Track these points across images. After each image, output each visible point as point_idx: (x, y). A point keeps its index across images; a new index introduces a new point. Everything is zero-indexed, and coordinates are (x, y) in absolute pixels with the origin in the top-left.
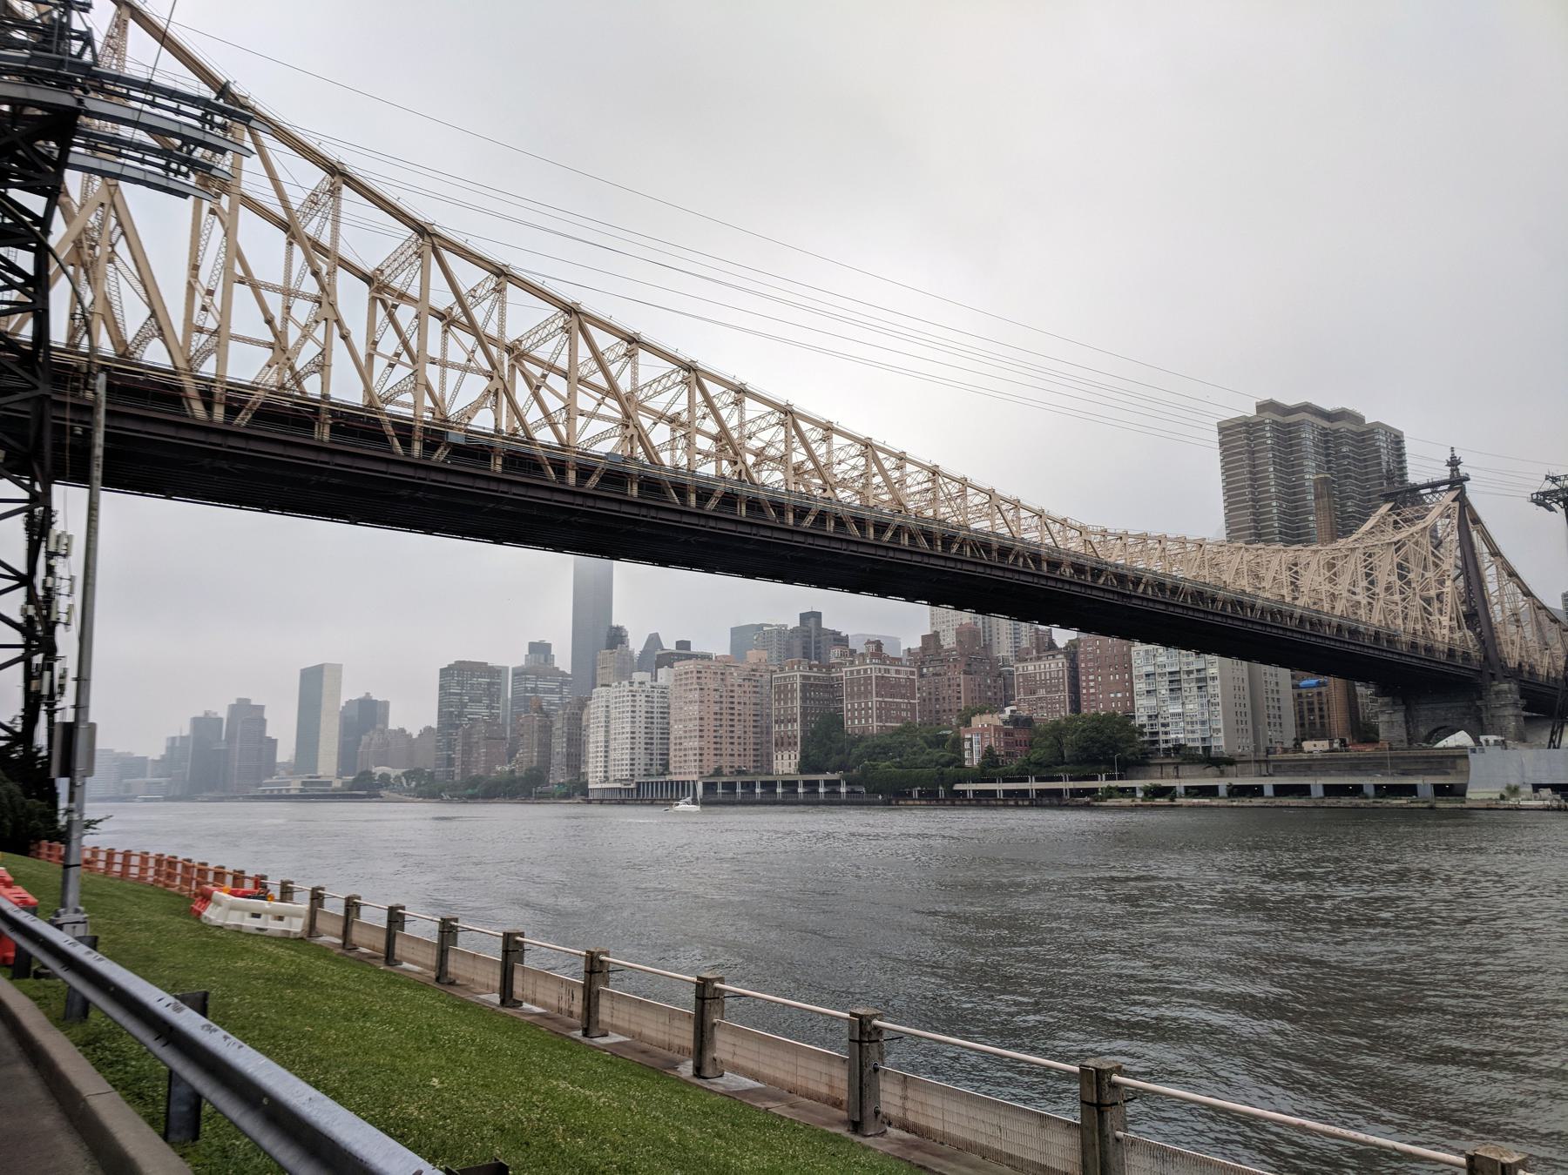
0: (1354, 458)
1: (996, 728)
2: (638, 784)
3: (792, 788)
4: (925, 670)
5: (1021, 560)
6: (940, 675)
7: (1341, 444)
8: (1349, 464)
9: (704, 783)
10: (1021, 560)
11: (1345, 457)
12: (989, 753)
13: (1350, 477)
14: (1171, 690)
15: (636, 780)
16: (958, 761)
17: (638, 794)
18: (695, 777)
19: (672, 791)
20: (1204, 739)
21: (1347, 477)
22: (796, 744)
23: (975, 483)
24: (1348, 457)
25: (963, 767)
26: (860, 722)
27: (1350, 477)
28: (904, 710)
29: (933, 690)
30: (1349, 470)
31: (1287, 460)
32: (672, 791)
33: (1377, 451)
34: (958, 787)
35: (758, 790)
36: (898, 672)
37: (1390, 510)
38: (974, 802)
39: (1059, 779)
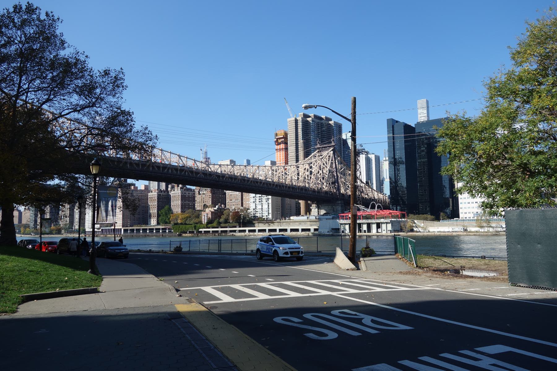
0: (327, 132)
1: (212, 212)
2: (102, 230)
3: (164, 230)
4: (200, 192)
5: (187, 173)
6: (205, 194)
7: (323, 127)
8: (325, 133)
9: (124, 229)
10: (187, 173)
11: (324, 131)
12: (208, 219)
13: (325, 137)
14: (259, 202)
15: (101, 228)
16: (201, 222)
17: (102, 233)
18: (121, 227)
19: (119, 231)
20: (267, 216)
21: (324, 137)
22: (155, 216)
23: (173, 152)
24: (324, 131)
25: (202, 224)
26: (176, 209)
27: (325, 137)
28: (190, 205)
29: (202, 199)
30: (325, 135)
31: (307, 132)
32: (119, 231)
33: (333, 130)
34: (200, 230)
35: (141, 232)
36: (189, 193)
37: (318, 152)
38: (204, 235)
39: (227, 227)
